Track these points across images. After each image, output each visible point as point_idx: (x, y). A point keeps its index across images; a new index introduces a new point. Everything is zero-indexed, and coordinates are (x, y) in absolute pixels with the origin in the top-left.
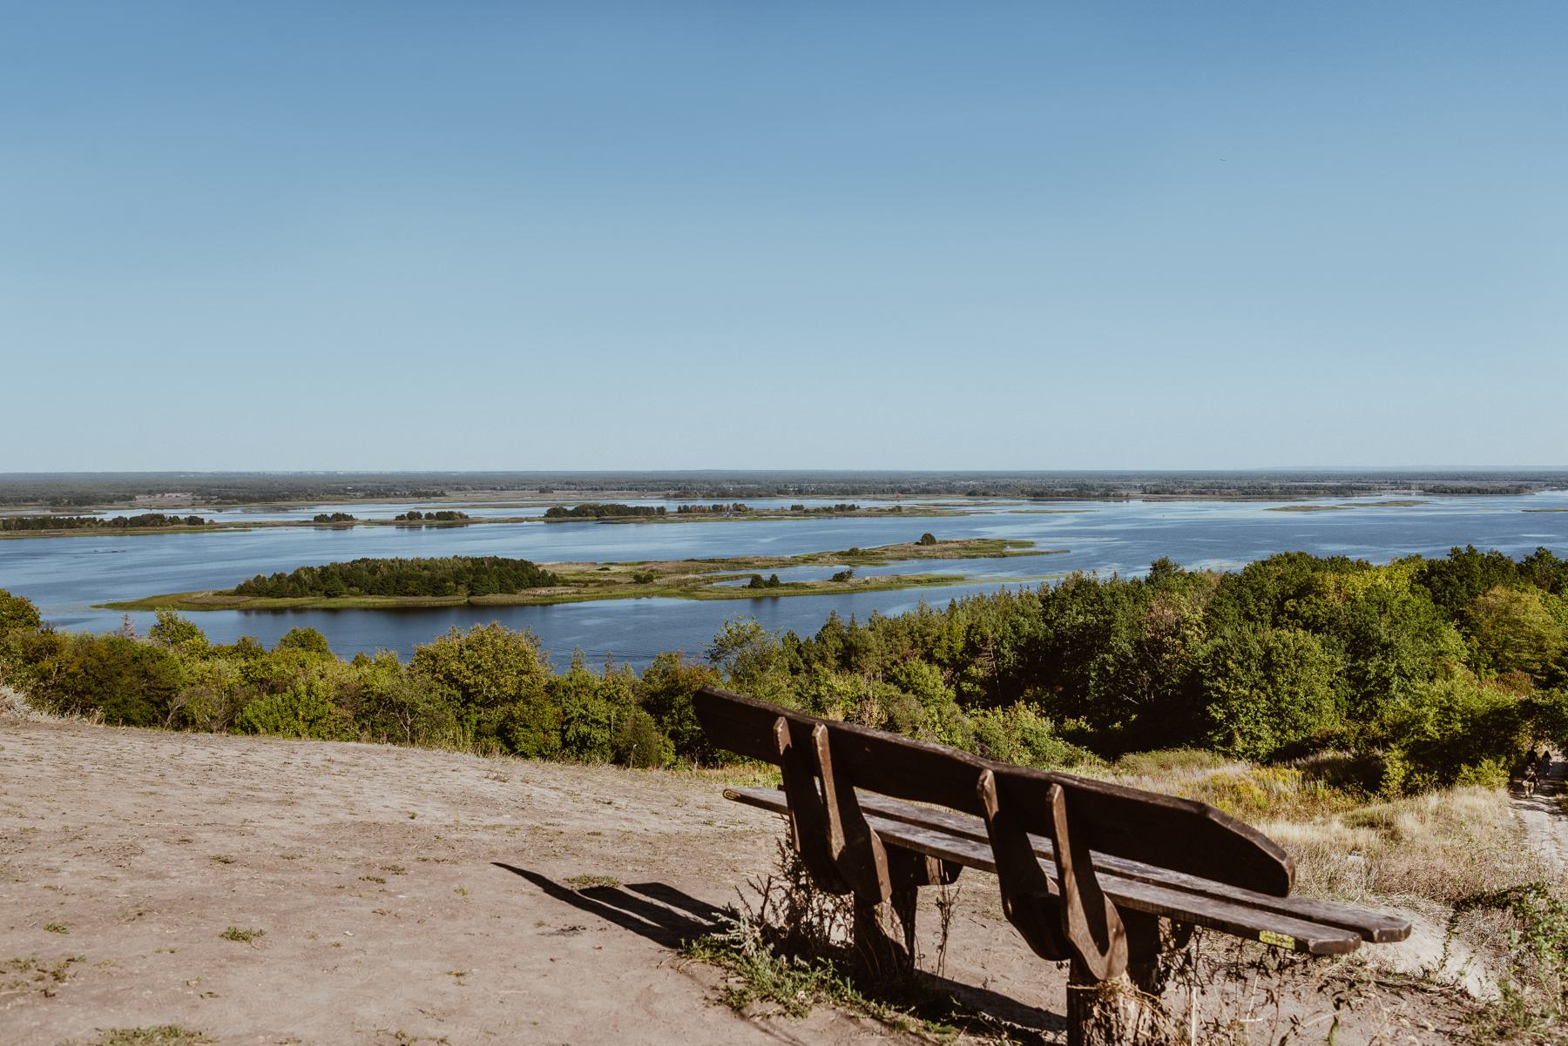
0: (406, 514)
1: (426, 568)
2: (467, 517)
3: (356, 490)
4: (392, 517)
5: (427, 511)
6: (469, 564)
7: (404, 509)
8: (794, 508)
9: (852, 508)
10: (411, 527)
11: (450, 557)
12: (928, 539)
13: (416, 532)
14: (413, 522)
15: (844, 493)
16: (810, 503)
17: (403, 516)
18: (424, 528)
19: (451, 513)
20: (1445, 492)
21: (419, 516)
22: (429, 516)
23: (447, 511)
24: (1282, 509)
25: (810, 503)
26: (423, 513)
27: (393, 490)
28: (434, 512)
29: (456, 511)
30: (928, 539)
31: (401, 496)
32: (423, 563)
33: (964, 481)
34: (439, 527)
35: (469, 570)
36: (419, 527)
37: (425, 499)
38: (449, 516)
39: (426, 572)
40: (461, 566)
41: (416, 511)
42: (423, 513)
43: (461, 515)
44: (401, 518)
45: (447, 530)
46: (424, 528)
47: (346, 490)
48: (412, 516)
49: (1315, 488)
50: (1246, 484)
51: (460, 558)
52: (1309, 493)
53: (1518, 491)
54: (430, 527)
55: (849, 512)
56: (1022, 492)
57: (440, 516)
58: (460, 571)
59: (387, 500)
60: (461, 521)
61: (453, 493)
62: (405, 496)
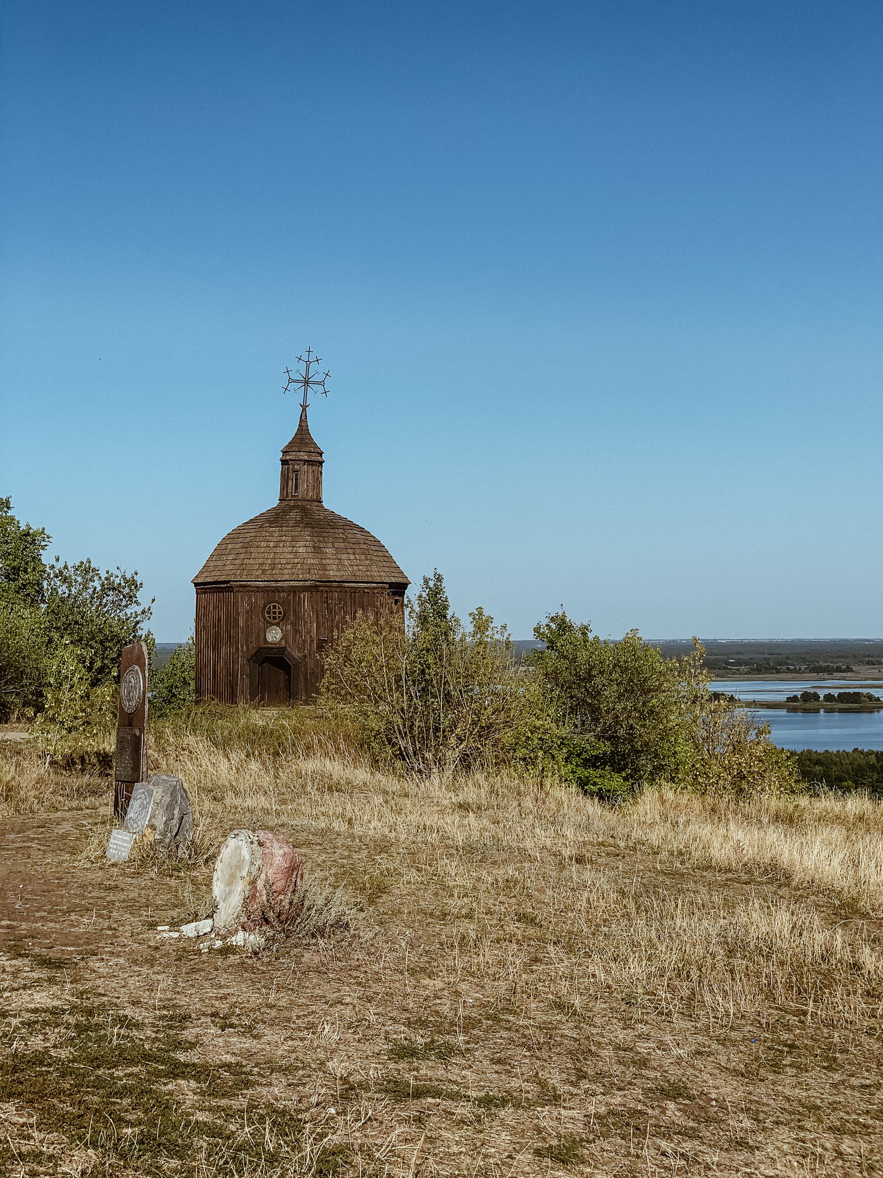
0: (799, 694)
1: (818, 762)
2: (878, 699)
3: (739, 663)
4: (782, 698)
5: (827, 692)
6: (873, 759)
7: (796, 688)
10: (805, 711)
11: (850, 750)
13: (811, 717)
14: (808, 705)
17: (795, 697)
18: (822, 712)
19: (858, 694)
21: (816, 697)
22: (829, 698)
23: (851, 691)
26: (822, 694)
27: (786, 664)
28: (835, 693)
29: (865, 691)
31: (795, 671)
32: (814, 757)
34: (841, 711)
35: (872, 767)
36: (817, 711)
37: (826, 676)
38: (855, 697)
39: (818, 768)
40: (863, 762)
41: (812, 691)
42: (822, 694)
43: (870, 697)
44: (794, 699)
45: (853, 716)
46: (822, 712)
47: (728, 663)
48: (808, 697)
51: (862, 752)
54: (829, 711)
57: (843, 698)
58: (861, 768)
59: (777, 676)
60: (870, 704)
61: (863, 668)
62: (799, 671)
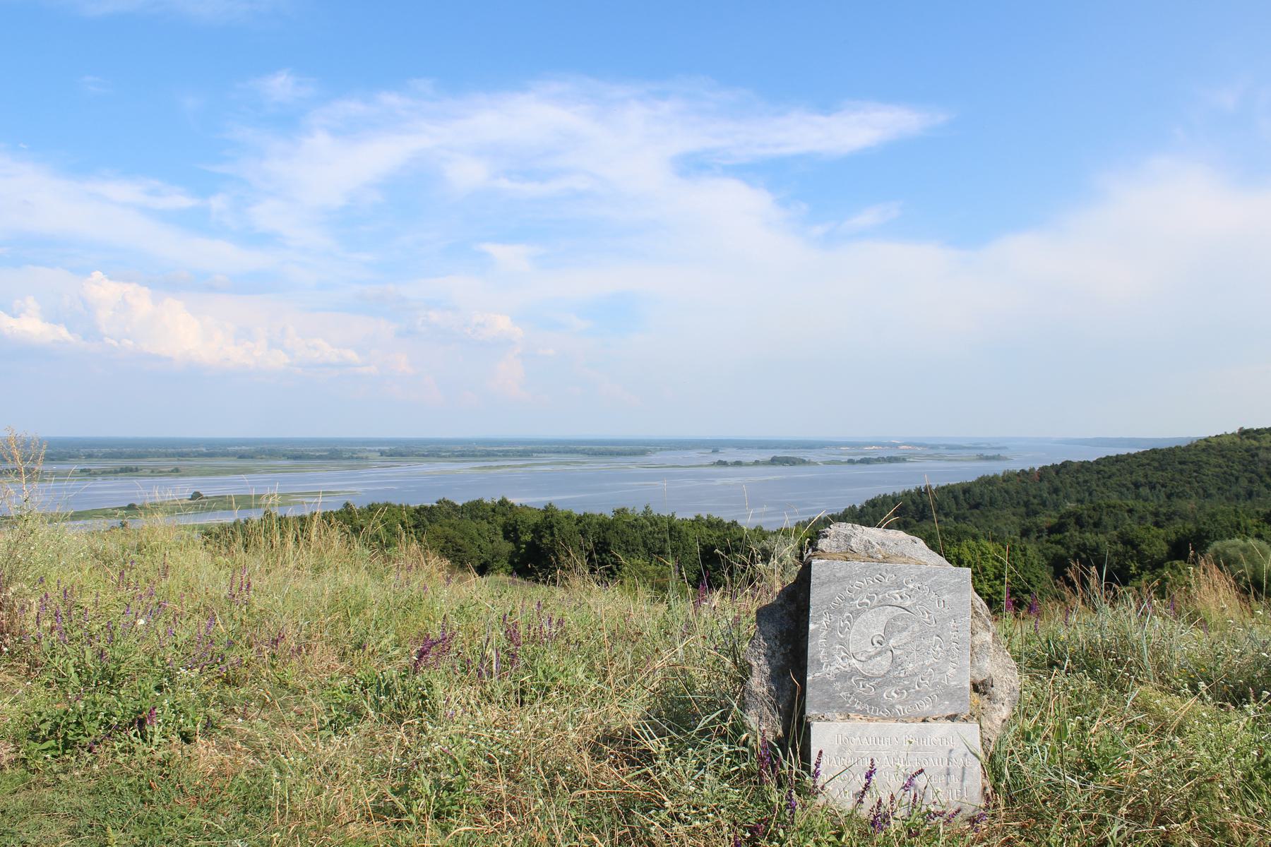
8: (82, 471)
9: (137, 470)
12: (196, 496)
15: (130, 456)
16: (95, 466)
20: (595, 455)
24: (479, 468)
25: (95, 466)
30: (196, 496)
33: (239, 446)
49: (508, 451)
50: (460, 449)
52: (504, 456)
53: (643, 453)
55: (135, 473)
56: (284, 456)
